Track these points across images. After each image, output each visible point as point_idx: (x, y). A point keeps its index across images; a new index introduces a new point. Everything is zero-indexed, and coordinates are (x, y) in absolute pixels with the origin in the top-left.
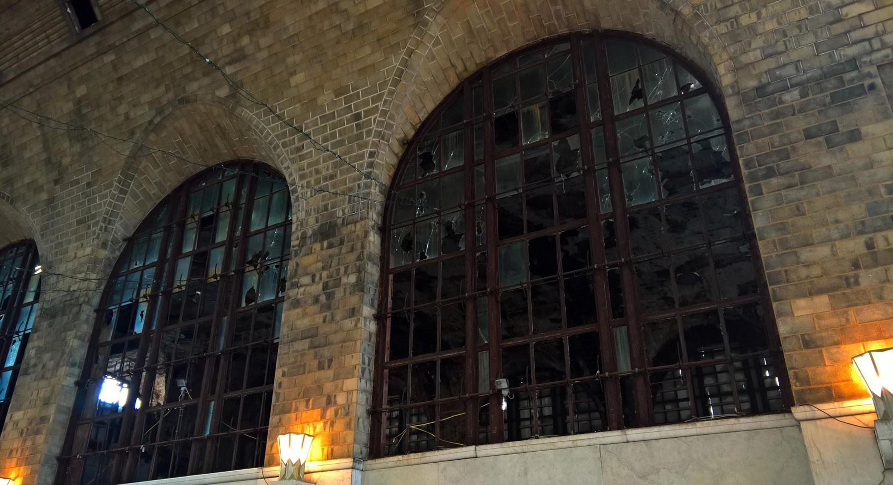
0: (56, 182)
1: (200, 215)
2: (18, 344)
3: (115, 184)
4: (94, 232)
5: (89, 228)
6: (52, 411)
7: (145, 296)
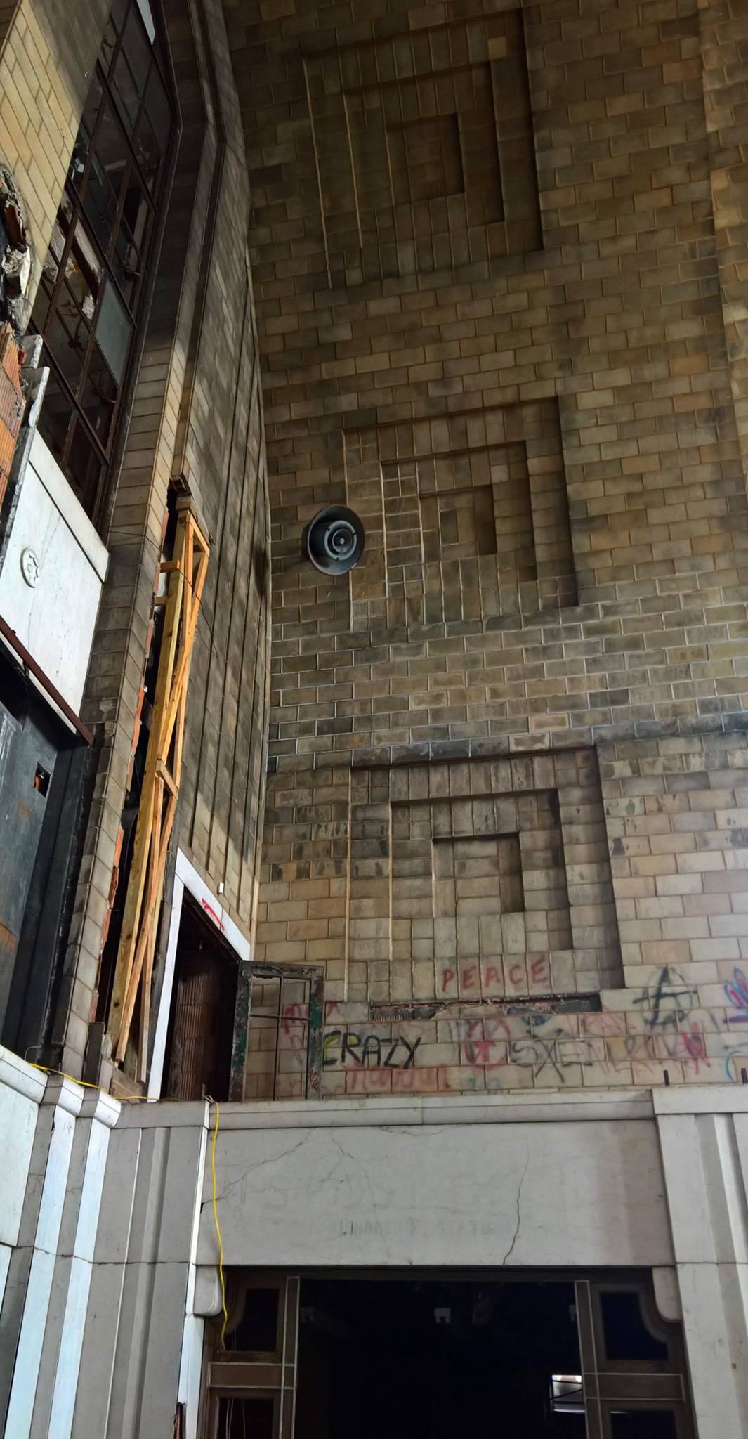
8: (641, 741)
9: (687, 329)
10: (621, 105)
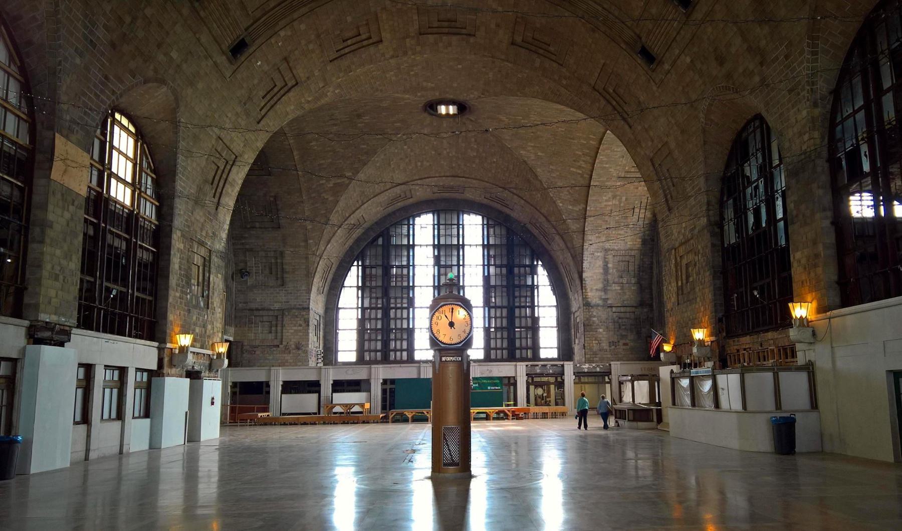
0: (761, 64)
1: (888, 49)
2: (780, 199)
3: (806, 49)
4: (804, 97)
5: (799, 94)
6: (820, 247)
7: (862, 139)
8: (290, 309)
9: (303, 244)
10: (292, 210)
